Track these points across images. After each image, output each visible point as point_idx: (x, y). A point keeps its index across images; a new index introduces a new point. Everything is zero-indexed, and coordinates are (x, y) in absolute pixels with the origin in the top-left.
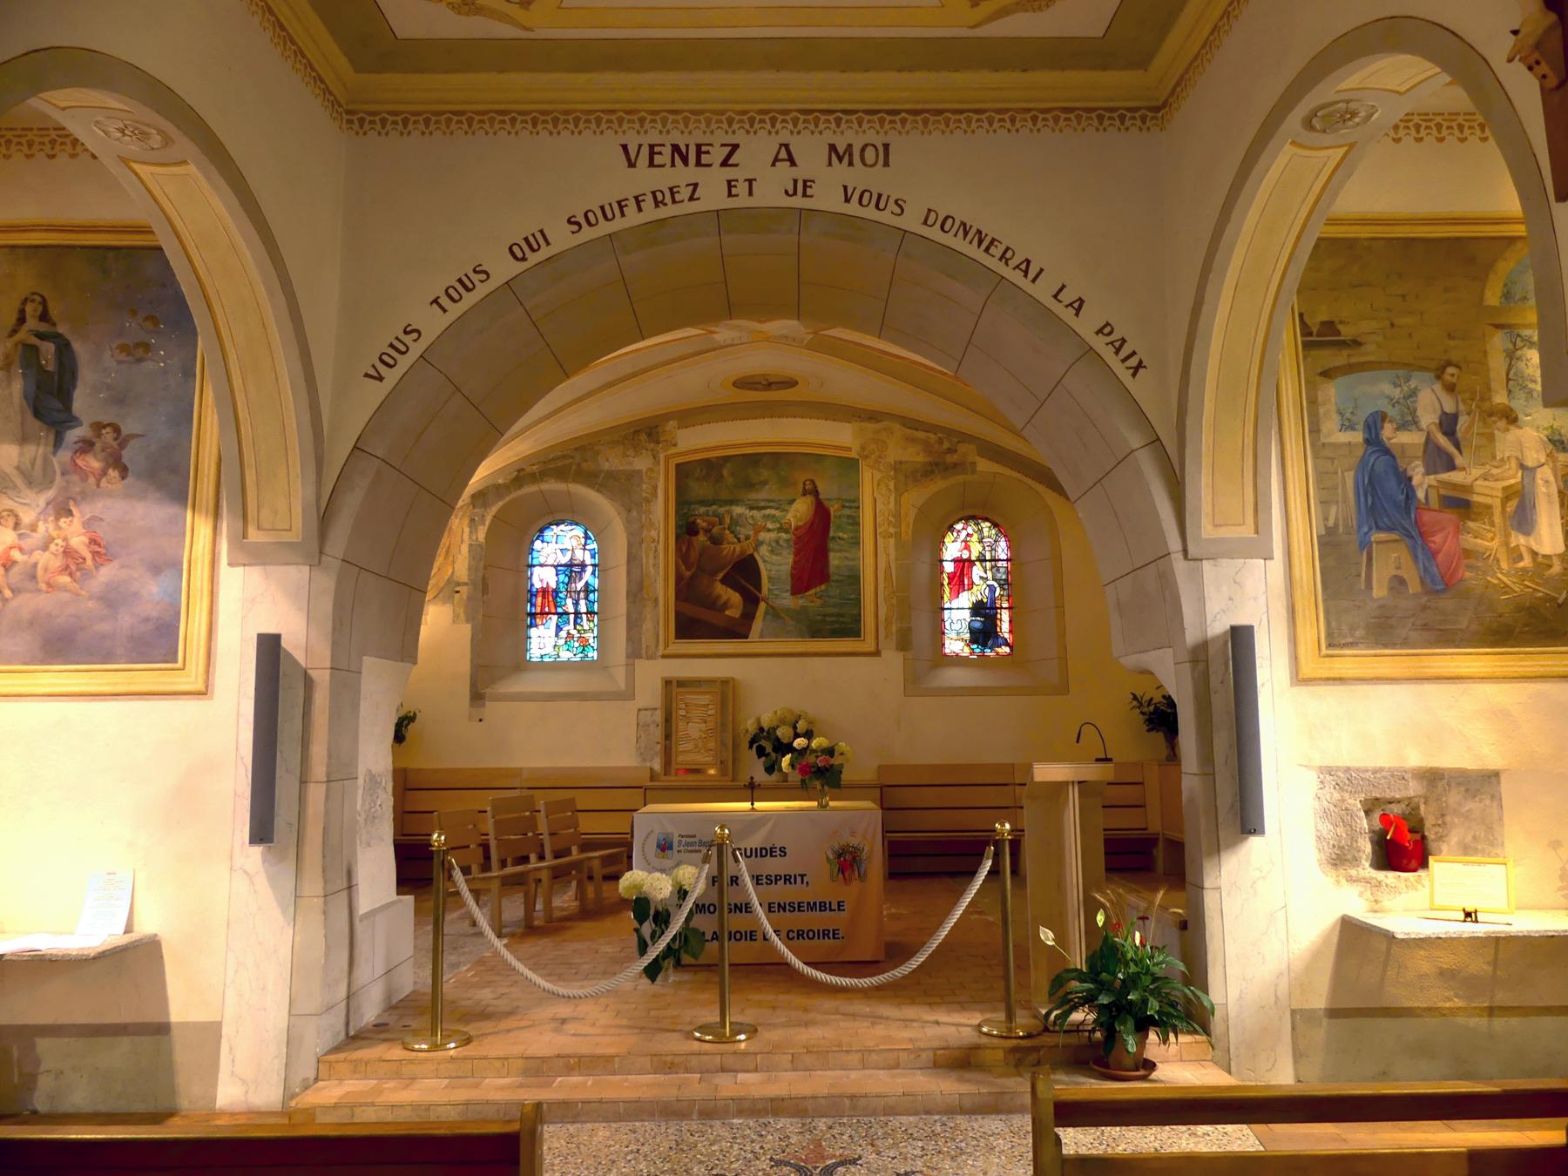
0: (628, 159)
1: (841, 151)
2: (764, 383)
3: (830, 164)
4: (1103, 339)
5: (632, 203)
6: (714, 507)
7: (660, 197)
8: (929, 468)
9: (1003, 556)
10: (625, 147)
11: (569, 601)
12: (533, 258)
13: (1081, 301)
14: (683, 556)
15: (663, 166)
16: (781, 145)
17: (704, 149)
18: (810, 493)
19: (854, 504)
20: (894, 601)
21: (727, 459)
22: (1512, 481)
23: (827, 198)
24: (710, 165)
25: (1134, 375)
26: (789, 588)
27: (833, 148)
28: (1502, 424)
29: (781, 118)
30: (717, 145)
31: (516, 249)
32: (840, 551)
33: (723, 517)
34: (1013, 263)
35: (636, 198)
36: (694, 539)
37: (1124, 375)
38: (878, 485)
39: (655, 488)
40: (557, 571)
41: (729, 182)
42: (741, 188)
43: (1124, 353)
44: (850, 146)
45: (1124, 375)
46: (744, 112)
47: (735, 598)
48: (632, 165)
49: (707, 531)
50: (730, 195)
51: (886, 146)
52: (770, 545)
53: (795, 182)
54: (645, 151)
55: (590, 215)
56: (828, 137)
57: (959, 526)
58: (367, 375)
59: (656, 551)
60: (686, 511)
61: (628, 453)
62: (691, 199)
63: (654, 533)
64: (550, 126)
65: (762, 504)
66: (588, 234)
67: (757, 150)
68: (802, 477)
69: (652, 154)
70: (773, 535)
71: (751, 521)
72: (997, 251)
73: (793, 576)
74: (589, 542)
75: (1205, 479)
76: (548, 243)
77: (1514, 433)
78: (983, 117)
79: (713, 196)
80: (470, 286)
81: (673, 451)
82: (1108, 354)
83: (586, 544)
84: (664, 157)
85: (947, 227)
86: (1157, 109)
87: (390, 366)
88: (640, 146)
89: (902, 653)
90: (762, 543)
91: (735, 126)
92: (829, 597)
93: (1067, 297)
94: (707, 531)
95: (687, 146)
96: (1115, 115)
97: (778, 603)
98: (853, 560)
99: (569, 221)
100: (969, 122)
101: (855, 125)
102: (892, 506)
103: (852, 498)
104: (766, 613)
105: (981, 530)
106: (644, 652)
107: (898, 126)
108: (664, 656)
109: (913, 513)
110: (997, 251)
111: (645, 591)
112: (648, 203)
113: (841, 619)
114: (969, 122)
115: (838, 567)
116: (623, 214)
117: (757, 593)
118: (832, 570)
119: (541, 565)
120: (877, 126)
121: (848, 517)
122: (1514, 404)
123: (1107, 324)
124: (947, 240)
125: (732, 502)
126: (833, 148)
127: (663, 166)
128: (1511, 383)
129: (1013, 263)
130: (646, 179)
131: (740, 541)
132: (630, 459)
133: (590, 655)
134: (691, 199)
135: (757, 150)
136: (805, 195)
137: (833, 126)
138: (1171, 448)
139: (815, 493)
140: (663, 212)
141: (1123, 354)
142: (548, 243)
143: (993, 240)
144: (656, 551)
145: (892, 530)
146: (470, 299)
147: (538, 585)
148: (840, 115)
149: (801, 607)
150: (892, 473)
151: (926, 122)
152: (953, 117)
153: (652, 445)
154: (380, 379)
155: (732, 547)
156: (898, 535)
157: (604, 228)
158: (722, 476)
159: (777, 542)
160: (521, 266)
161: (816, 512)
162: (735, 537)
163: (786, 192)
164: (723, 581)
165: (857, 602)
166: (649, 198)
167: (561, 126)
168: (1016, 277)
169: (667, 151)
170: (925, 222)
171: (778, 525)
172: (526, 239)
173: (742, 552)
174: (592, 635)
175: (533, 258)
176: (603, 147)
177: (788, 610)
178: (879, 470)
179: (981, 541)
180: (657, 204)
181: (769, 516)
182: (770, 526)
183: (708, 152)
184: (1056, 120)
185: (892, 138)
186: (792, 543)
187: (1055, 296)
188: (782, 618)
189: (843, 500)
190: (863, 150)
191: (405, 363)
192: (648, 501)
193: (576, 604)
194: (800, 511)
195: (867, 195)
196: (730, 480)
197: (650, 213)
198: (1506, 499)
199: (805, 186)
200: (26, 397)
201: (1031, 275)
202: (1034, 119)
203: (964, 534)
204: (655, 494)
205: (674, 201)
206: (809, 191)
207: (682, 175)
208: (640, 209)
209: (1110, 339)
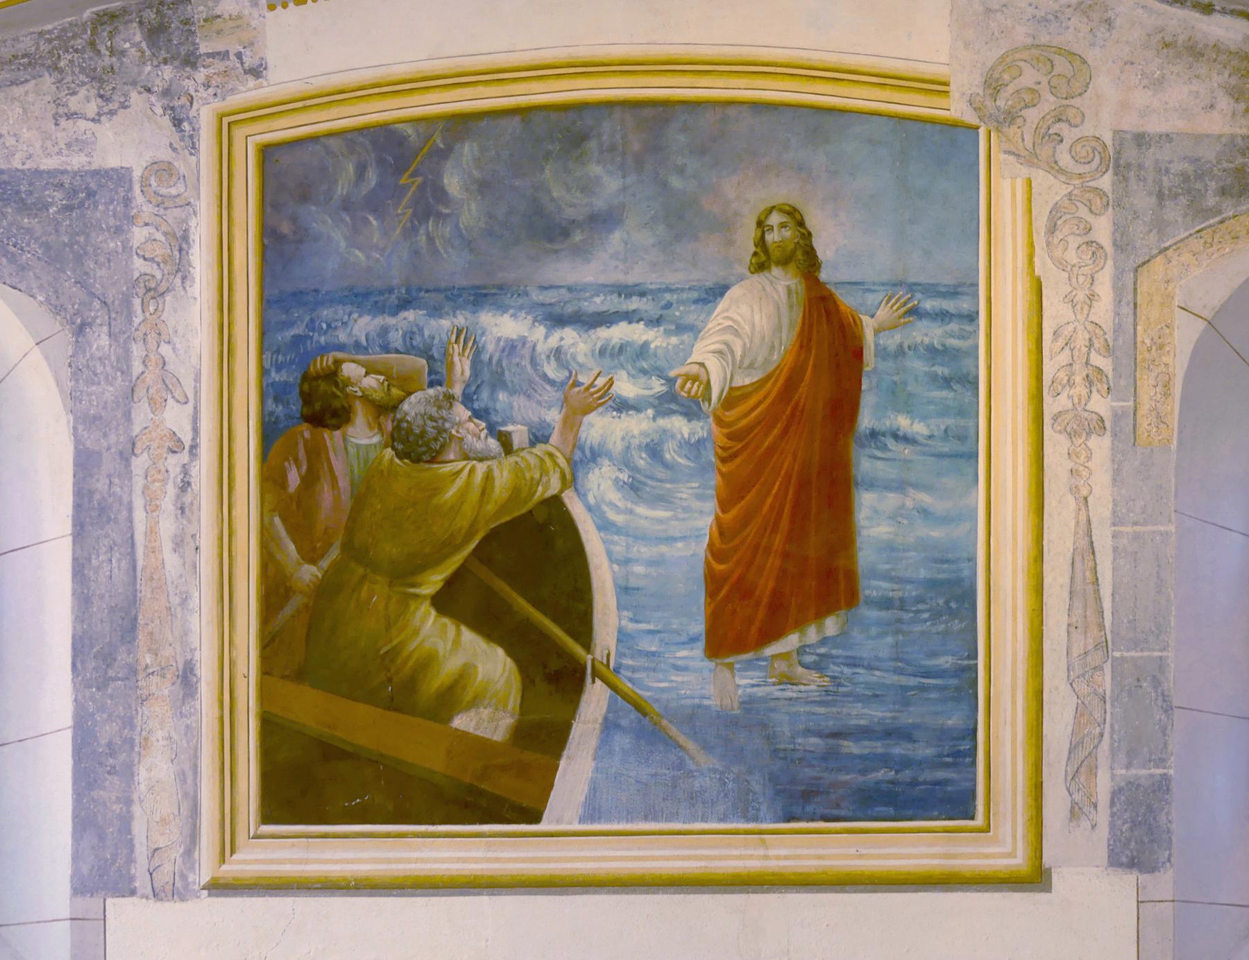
6: (410, 315)
18: (784, 262)
20: (1106, 681)
32: (901, 486)
36: (332, 438)
38: (1052, 229)
49: (383, 409)
60: (295, 331)
61: (74, 103)
65: (599, 303)
71: (551, 370)
73: (714, 582)
81: (248, 93)
89: (1129, 879)
90: (596, 455)
92: (853, 662)
94: (383, 409)
98: (945, 520)
102: (1104, 310)
106: (140, 870)
108: (218, 887)
111: (142, 637)
113: (899, 749)
115: (890, 548)
117: (578, 650)
118: (866, 556)
121: (933, 353)
144: (185, 486)
149: (748, 704)
150: (1106, 182)
153: (168, 72)
155: (481, 468)
158: (441, 194)
161: (805, 341)
164: (443, 602)
171: (658, 386)
173: (516, 494)
177: (692, 718)
178: (1055, 168)
181: (622, 348)
182: (626, 387)
186: (710, 456)
189: (912, 287)
192: (155, 292)
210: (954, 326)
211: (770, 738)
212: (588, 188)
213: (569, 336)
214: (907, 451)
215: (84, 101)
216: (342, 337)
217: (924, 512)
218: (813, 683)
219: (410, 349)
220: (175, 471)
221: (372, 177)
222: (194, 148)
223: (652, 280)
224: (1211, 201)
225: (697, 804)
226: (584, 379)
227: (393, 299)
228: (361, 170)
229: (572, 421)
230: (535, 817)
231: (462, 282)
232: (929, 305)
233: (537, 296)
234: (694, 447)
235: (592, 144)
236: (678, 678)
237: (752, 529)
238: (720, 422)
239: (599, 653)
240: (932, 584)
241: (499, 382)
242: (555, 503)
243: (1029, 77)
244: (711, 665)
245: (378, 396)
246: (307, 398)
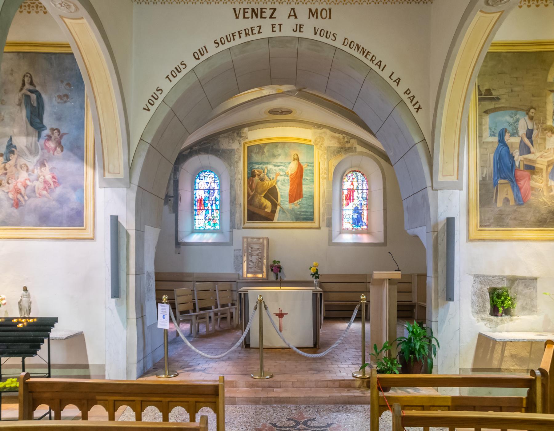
2: (280, 111)
6: (261, 165)
11: (209, 205)
14: (250, 186)
18: (296, 160)
21: (266, 144)
26: (288, 200)
36: (254, 179)
40: (205, 192)
47: (268, 204)
59: (240, 184)
63: (239, 176)
65: (279, 164)
68: (293, 153)
73: (289, 195)
81: (246, 141)
90: (278, 181)
92: (302, 204)
94: (259, 175)
97: (283, 206)
98: (311, 188)
104: (280, 211)
108: (243, 228)
111: (236, 200)
115: (306, 191)
117: (277, 202)
118: (304, 192)
119: (199, 189)
125: (268, 163)
132: (230, 144)
133: (217, 227)
139: (298, 160)
144: (240, 184)
147: (198, 198)
149: (293, 208)
155: (268, 182)
158: (264, 152)
159: (284, 180)
164: (265, 197)
165: (312, 206)
171: (284, 173)
173: (271, 185)
174: (217, 219)
177: (287, 210)
181: (281, 169)
182: (281, 173)
186: (289, 181)
188: (285, 213)
192: (237, 162)
193: (212, 205)
194: (292, 168)
196: (267, 154)
204: (240, 159)
211: (295, 212)
213: (276, 168)
214: (307, 181)
215: (231, 141)
217: (309, 188)
218: (299, 206)
219: (261, 169)
220: (239, 182)
221: (258, 150)
223: (284, 162)
225: (288, 219)
226: (278, 172)
227: (260, 163)
228: (257, 149)
229: (276, 177)
230: (273, 221)
231: (266, 162)
235: (278, 147)
236: (286, 205)
237: (293, 189)
238: (290, 177)
239: (279, 203)
240: (310, 195)
241: (269, 173)
242: (275, 186)
244: (289, 204)
246: (252, 174)
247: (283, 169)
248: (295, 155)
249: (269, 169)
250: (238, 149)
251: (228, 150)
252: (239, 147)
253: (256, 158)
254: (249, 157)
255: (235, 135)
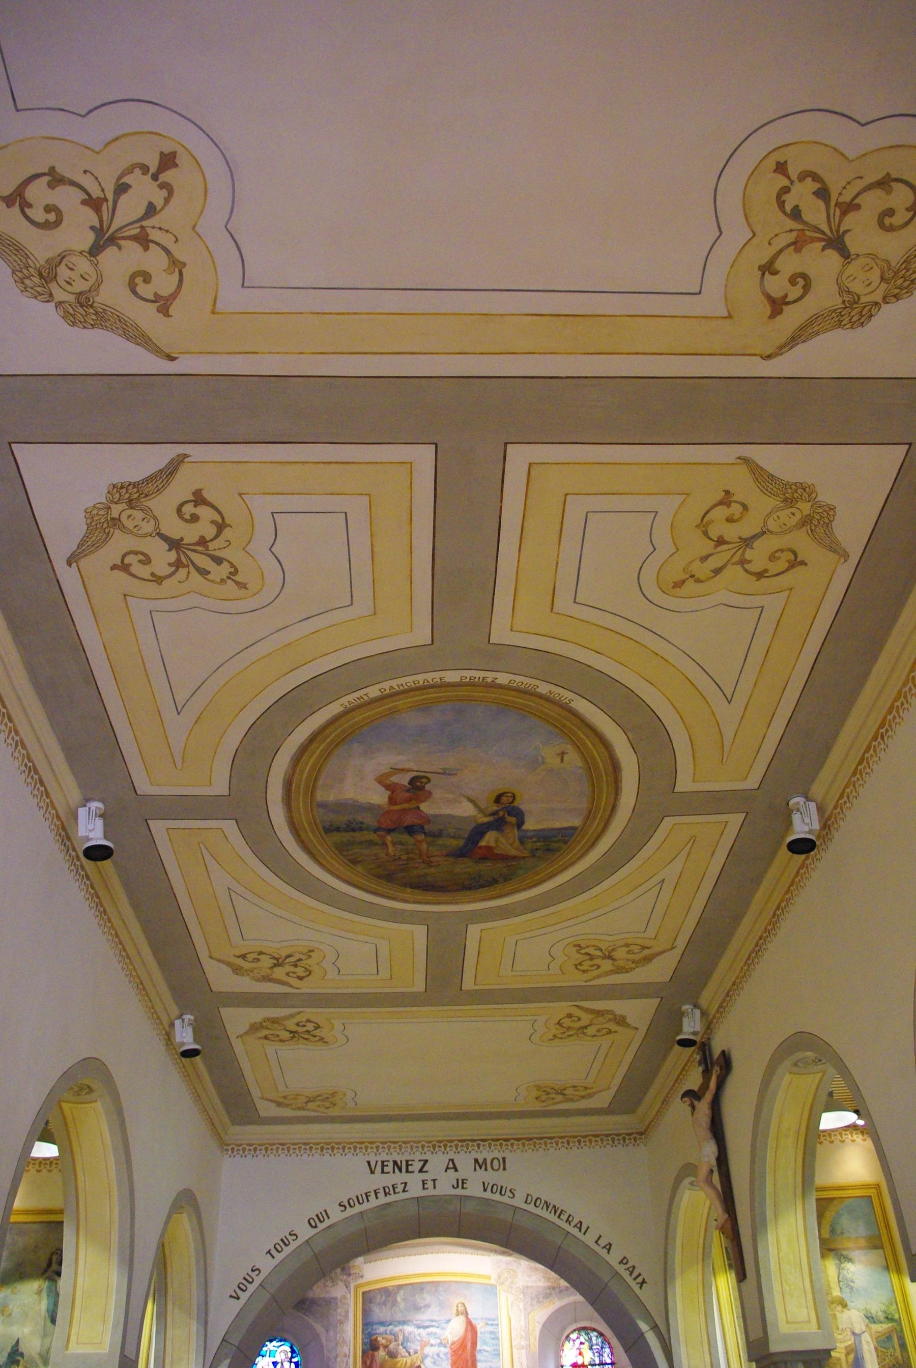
0: (371, 1169)
1: (481, 1162)
3: (475, 1170)
4: (623, 1267)
5: (373, 1194)
6: (391, 1327)
7: (387, 1190)
8: (548, 1291)
9: (609, 1361)
10: (369, 1163)
12: (321, 1226)
13: (610, 1245)
15: (389, 1173)
16: (450, 1160)
17: (410, 1163)
18: (462, 1314)
19: (493, 1322)
21: (400, 1287)
22: (849, 1343)
23: (474, 1189)
24: (413, 1172)
25: (641, 1288)
27: (476, 1161)
28: (839, 1308)
29: (449, 1144)
30: (417, 1160)
31: (312, 1221)
32: (486, 1361)
33: (398, 1335)
34: (573, 1224)
35: (375, 1191)
36: (376, 1353)
37: (636, 1288)
38: (512, 1306)
39: (347, 1312)
41: (423, 1181)
42: (430, 1184)
43: (634, 1275)
44: (485, 1159)
45: (636, 1288)
46: (430, 1142)
48: (372, 1172)
50: (424, 1188)
51: (504, 1159)
52: (433, 1358)
53: (458, 1180)
54: (379, 1164)
55: (351, 1201)
56: (474, 1155)
57: (574, 1336)
58: (231, 1296)
60: (370, 1330)
61: (327, 1284)
62: (404, 1191)
63: (346, 1350)
64: (330, 1151)
65: (427, 1324)
66: (350, 1212)
67: (437, 1162)
68: (455, 1301)
69: (383, 1166)
70: (435, 1350)
71: (418, 1338)
72: (564, 1217)
74: (294, 1355)
75: (683, 1349)
76: (328, 1218)
77: (846, 1312)
78: (553, 1141)
79: (415, 1190)
80: (287, 1243)
81: (360, 1281)
82: (625, 1275)
83: (292, 1357)
84: (389, 1169)
85: (537, 1204)
86: (641, 1134)
87: (244, 1291)
88: (377, 1162)
90: (426, 1356)
91: (426, 1149)
93: (603, 1242)
94: (386, 1347)
95: (401, 1162)
96: (620, 1138)
99: (340, 1205)
100: (546, 1144)
101: (488, 1148)
102: (522, 1323)
103: (493, 1317)
105: (590, 1339)
107: (510, 1147)
109: (538, 1328)
110: (564, 1217)
112: (381, 1195)
114: (546, 1144)
116: (368, 1201)
120: (498, 1147)
121: (491, 1333)
122: (844, 1296)
123: (625, 1258)
124: (537, 1211)
125: (404, 1323)
126: (476, 1161)
127: (389, 1173)
128: (841, 1283)
129: (573, 1224)
130: (380, 1180)
131: (410, 1355)
132: (328, 1288)
134: (404, 1191)
135: (437, 1162)
136: (463, 1188)
137: (476, 1148)
138: (664, 1332)
140: (389, 1199)
141: (634, 1275)
142: (328, 1218)
143: (562, 1211)
144: (347, 1364)
145: (523, 1343)
146: (287, 1250)
148: (479, 1142)
150: (521, 1296)
151: (524, 1145)
152: (538, 1141)
153: (345, 1277)
154: (238, 1298)
155: (405, 1359)
156: (528, 1348)
157: (358, 1208)
158: (396, 1301)
159: (438, 1355)
160: (314, 1231)
161: (466, 1331)
162: (407, 1351)
163: (453, 1186)
166: (381, 1191)
167: (335, 1151)
168: (575, 1231)
169: (391, 1164)
170: (526, 1202)
171: (439, 1341)
172: (317, 1216)
175: (321, 1226)
176: (358, 1162)
179: (591, 1348)
180: (386, 1194)
182: (433, 1341)
183: (412, 1165)
184: (590, 1141)
185: (507, 1154)
186: (449, 1356)
187: (596, 1242)
189: (486, 1319)
190: (492, 1162)
191: (251, 1288)
192: (341, 1322)
194: (455, 1329)
195: (495, 1187)
196: (402, 1305)
197: (383, 1200)
198: (848, 1354)
199: (463, 1183)
200: (48, 1311)
201: (583, 1230)
202: (579, 1142)
203: (578, 1342)
204: (347, 1316)
205: (395, 1193)
206: (465, 1185)
207: (399, 1178)
208: (377, 1198)
209: (627, 1266)
210: (494, 1327)
212: (424, 1299)
213: (421, 1330)
214: (485, 1353)
215: (329, 1283)
216: (378, 1331)
219: (391, 1334)
221: (384, 1298)
222: (350, 1293)
223: (437, 1319)
224: (541, 1299)
226: (424, 1340)
229: (422, 1349)
231: (401, 1320)
232: (490, 1322)
233: (415, 1322)
234: (446, 1354)
241: (408, 1341)
243: (506, 1275)
245: (385, 1344)
246: (371, 1344)
247: (435, 1334)
248: (460, 1305)
249: (406, 1334)
250: (344, 1297)
251: (324, 1299)
252: (344, 1294)
253: (379, 1313)
254: (366, 1312)
255: (338, 1271)
